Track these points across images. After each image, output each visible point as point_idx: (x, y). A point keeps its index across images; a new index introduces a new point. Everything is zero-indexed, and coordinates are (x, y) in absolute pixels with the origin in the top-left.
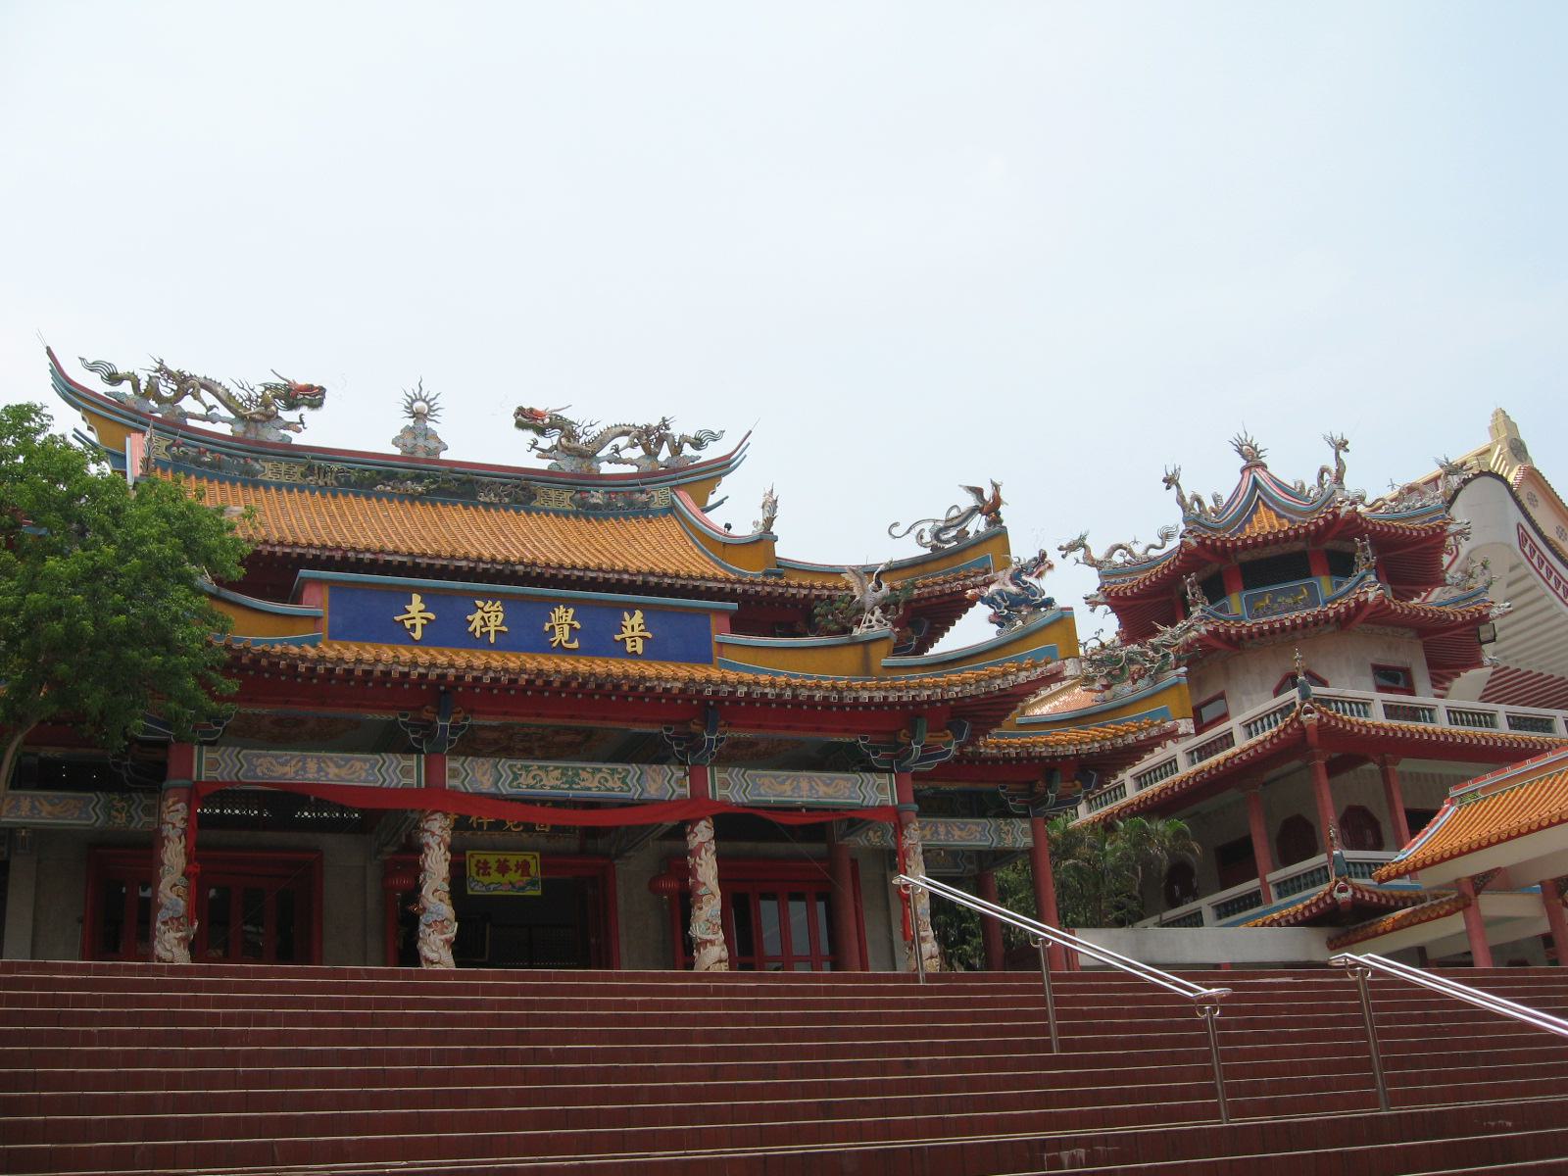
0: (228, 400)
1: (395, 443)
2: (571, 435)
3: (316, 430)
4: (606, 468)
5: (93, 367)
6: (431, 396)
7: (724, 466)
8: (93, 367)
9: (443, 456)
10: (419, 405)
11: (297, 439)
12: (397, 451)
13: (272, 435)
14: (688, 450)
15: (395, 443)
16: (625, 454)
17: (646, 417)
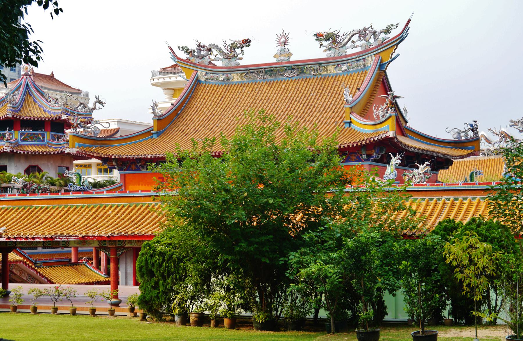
0: (220, 51)
1: (275, 56)
2: (334, 42)
3: (249, 57)
4: (350, 52)
5: (181, 49)
6: (287, 35)
7: (401, 38)
8: (181, 49)
9: (292, 59)
10: (283, 40)
11: (242, 63)
12: (274, 60)
13: (233, 63)
14: (383, 35)
15: (275, 56)
16: (357, 44)
17: (360, 27)
